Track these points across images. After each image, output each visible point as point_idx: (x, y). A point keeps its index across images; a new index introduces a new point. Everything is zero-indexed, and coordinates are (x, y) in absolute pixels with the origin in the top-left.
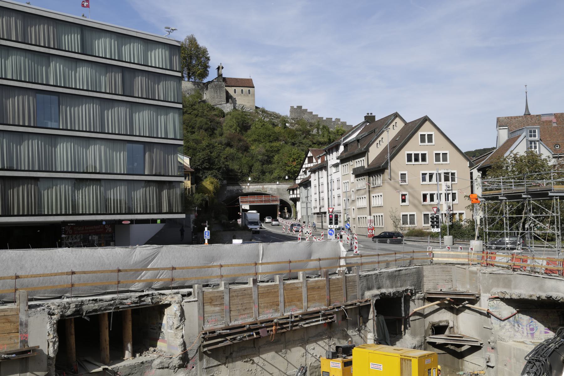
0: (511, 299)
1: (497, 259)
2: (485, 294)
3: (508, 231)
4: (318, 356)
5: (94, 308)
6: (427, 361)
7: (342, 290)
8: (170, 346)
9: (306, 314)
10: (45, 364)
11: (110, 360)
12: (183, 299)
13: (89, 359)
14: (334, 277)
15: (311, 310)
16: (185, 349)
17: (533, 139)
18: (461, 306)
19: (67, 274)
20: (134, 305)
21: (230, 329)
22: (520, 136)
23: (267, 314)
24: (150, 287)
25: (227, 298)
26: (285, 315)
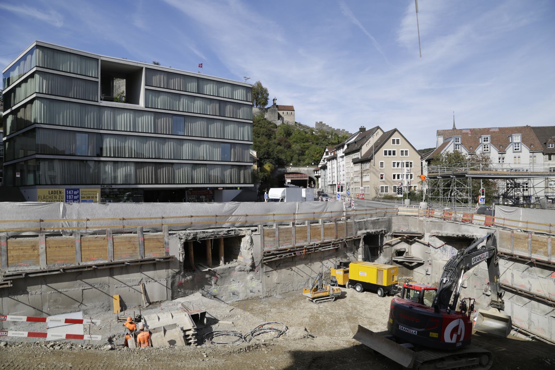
0: (442, 236)
1: (435, 213)
2: (427, 234)
3: (442, 197)
4: (330, 267)
5: (203, 236)
6: (392, 271)
7: (344, 230)
8: (245, 259)
9: (323, 244)
10: (178, 265)
11: (212, 265)
12: (252, 233)
13: (201, 264)
14: (339, 222)
15: (326, 241)
16: (253, 261)
17: (457, 143)
18: (413, 240)
19: (189, 217)
20: (225, 235)
21: (279, 251)
22: (450, 141)
23: (300, 243)
24: (233, 225)
25: (277, 233)
26: (311, 243)
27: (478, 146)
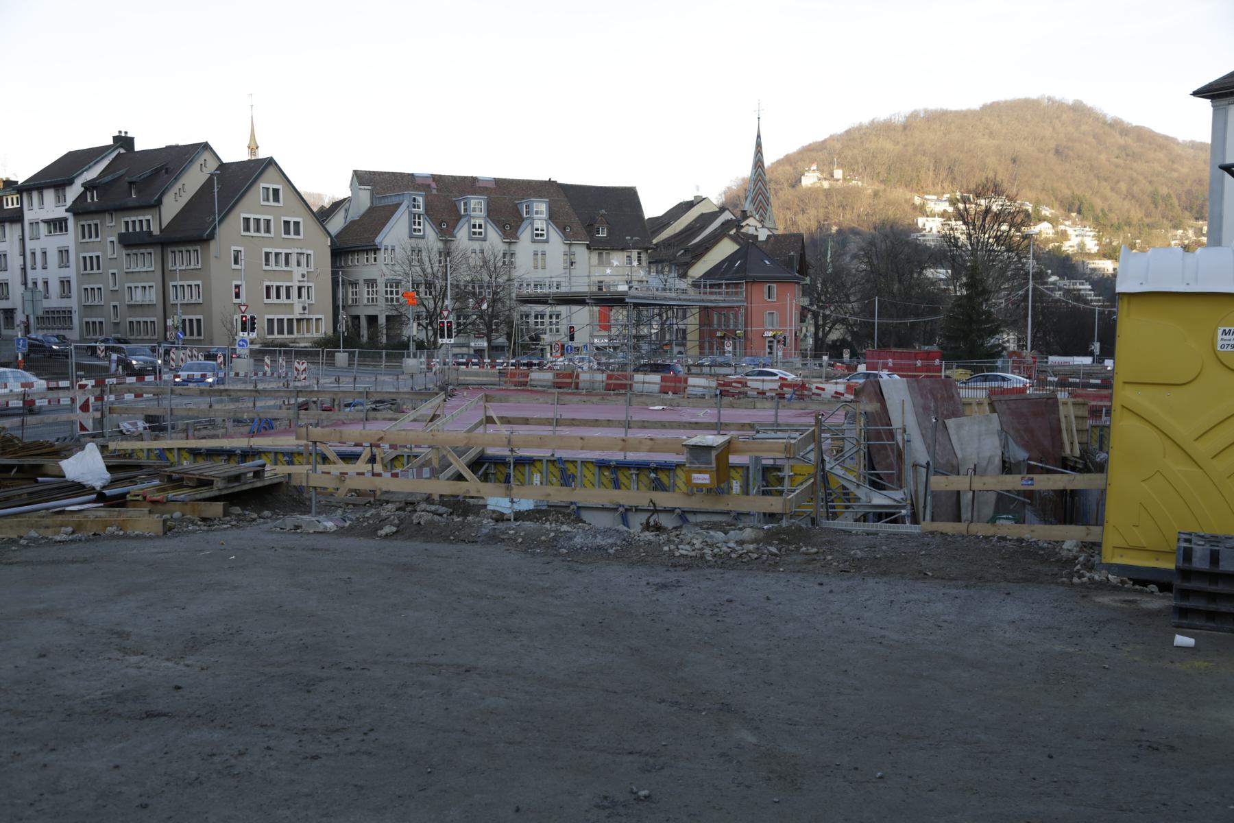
22: (401, 204)
27: (458, 221)
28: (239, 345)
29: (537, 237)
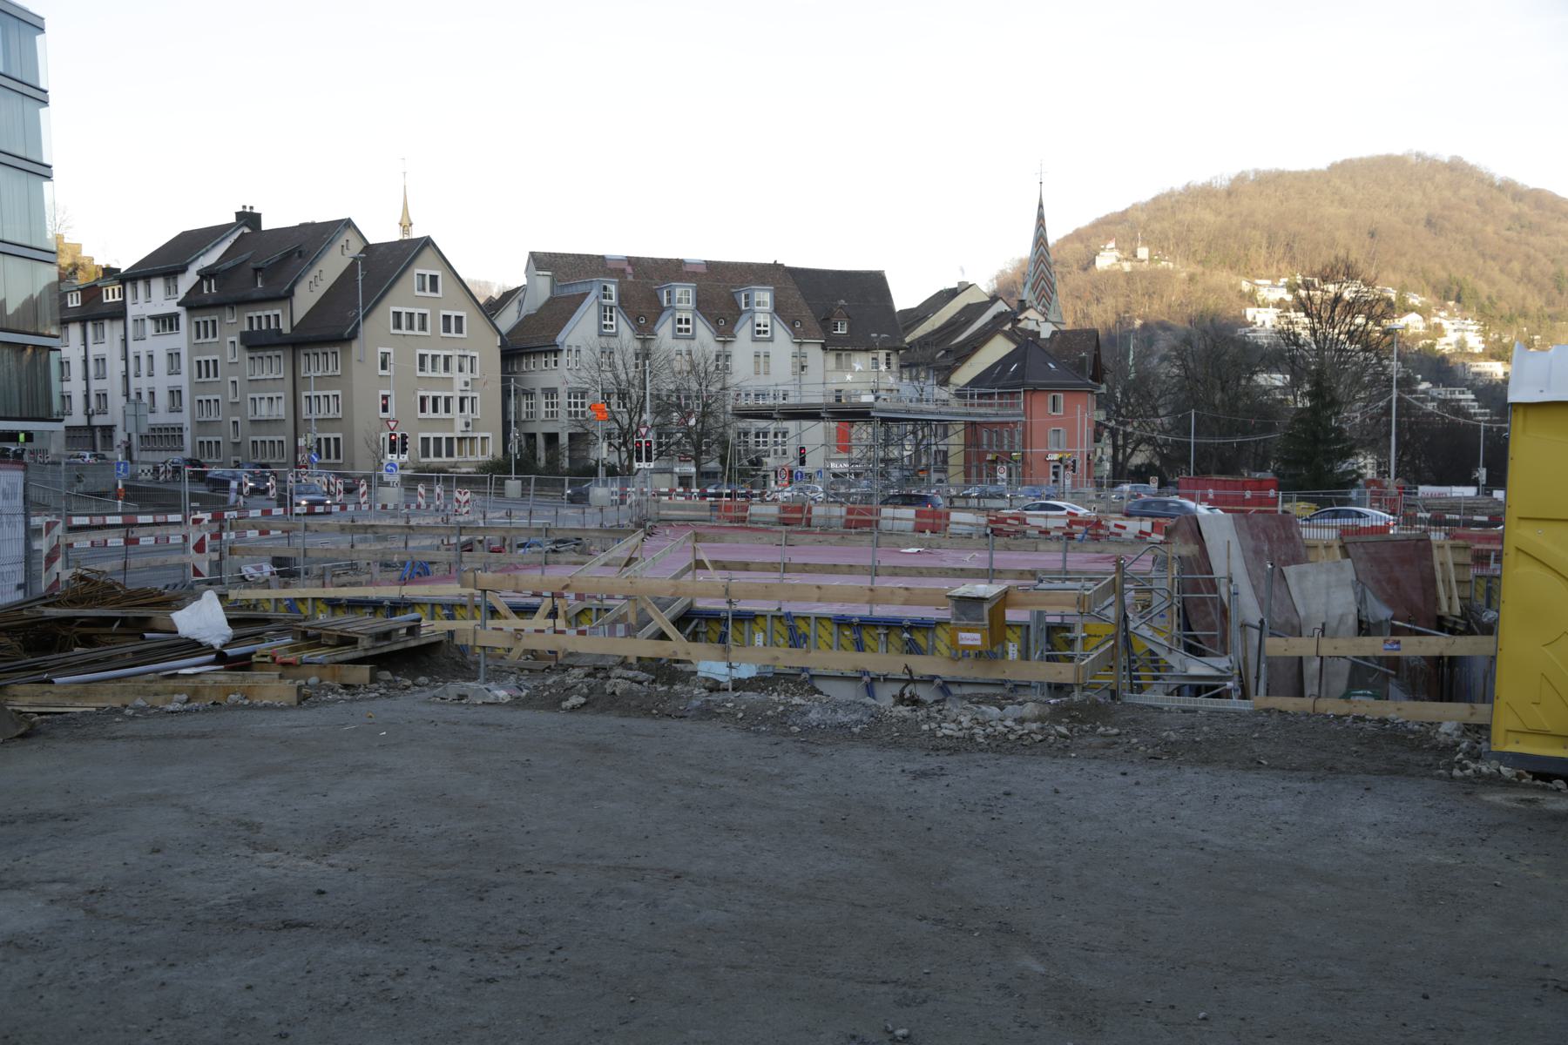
28: (387, 470)
29: (759, 334)
